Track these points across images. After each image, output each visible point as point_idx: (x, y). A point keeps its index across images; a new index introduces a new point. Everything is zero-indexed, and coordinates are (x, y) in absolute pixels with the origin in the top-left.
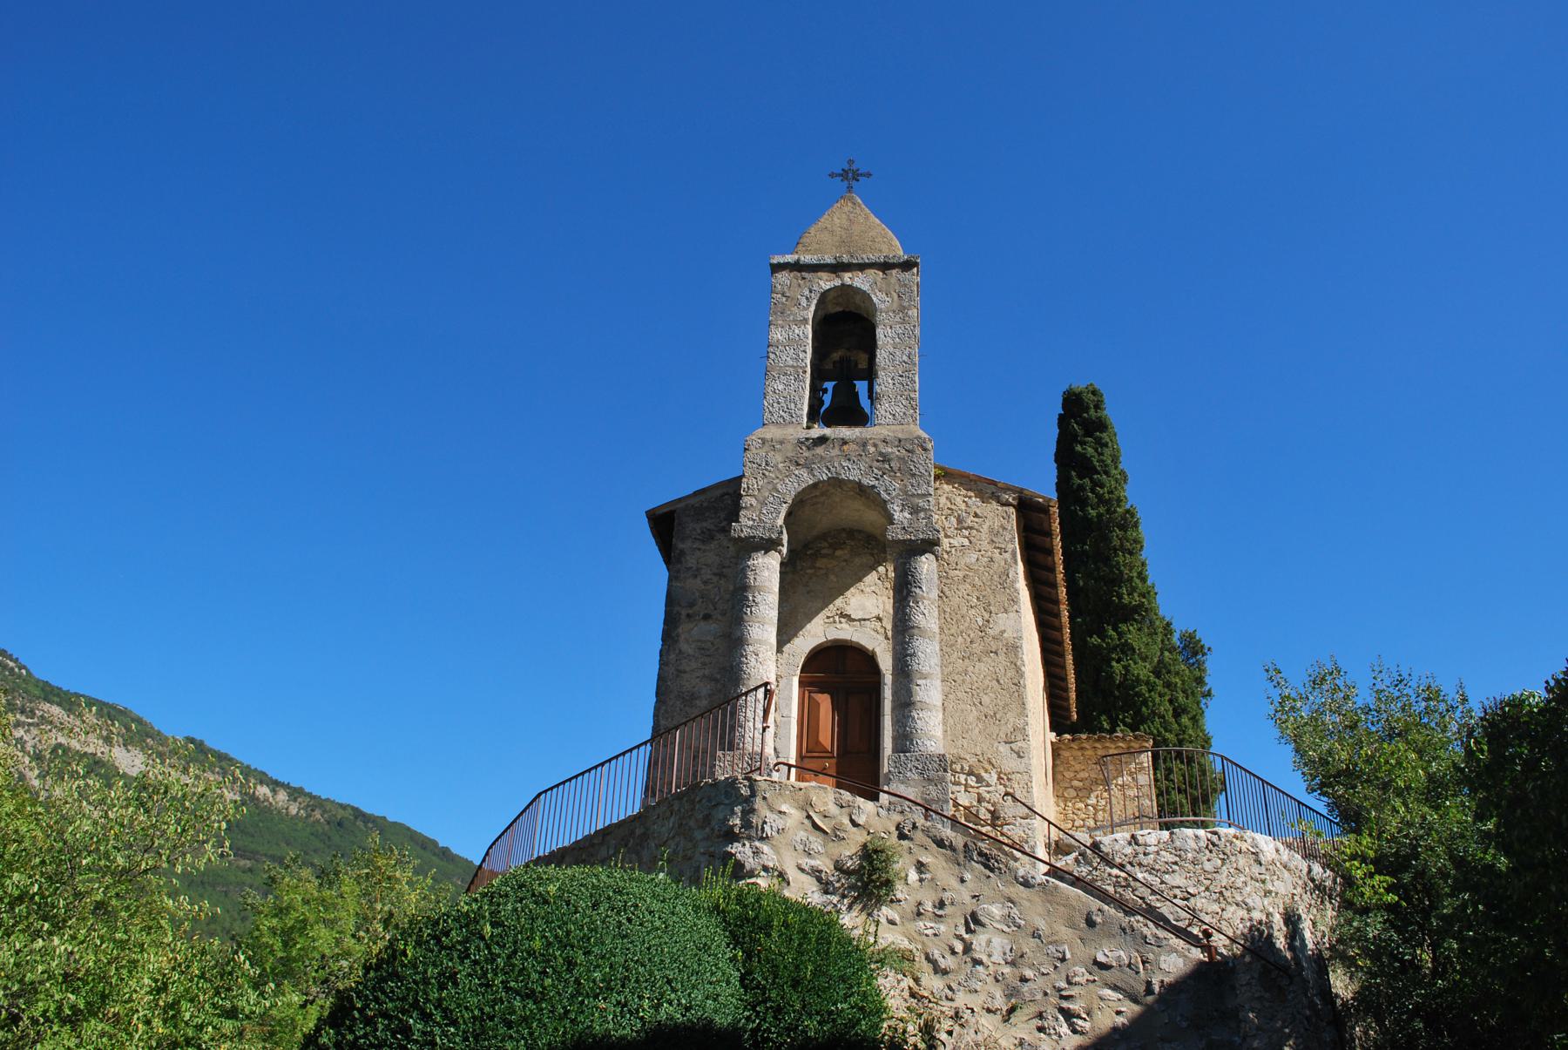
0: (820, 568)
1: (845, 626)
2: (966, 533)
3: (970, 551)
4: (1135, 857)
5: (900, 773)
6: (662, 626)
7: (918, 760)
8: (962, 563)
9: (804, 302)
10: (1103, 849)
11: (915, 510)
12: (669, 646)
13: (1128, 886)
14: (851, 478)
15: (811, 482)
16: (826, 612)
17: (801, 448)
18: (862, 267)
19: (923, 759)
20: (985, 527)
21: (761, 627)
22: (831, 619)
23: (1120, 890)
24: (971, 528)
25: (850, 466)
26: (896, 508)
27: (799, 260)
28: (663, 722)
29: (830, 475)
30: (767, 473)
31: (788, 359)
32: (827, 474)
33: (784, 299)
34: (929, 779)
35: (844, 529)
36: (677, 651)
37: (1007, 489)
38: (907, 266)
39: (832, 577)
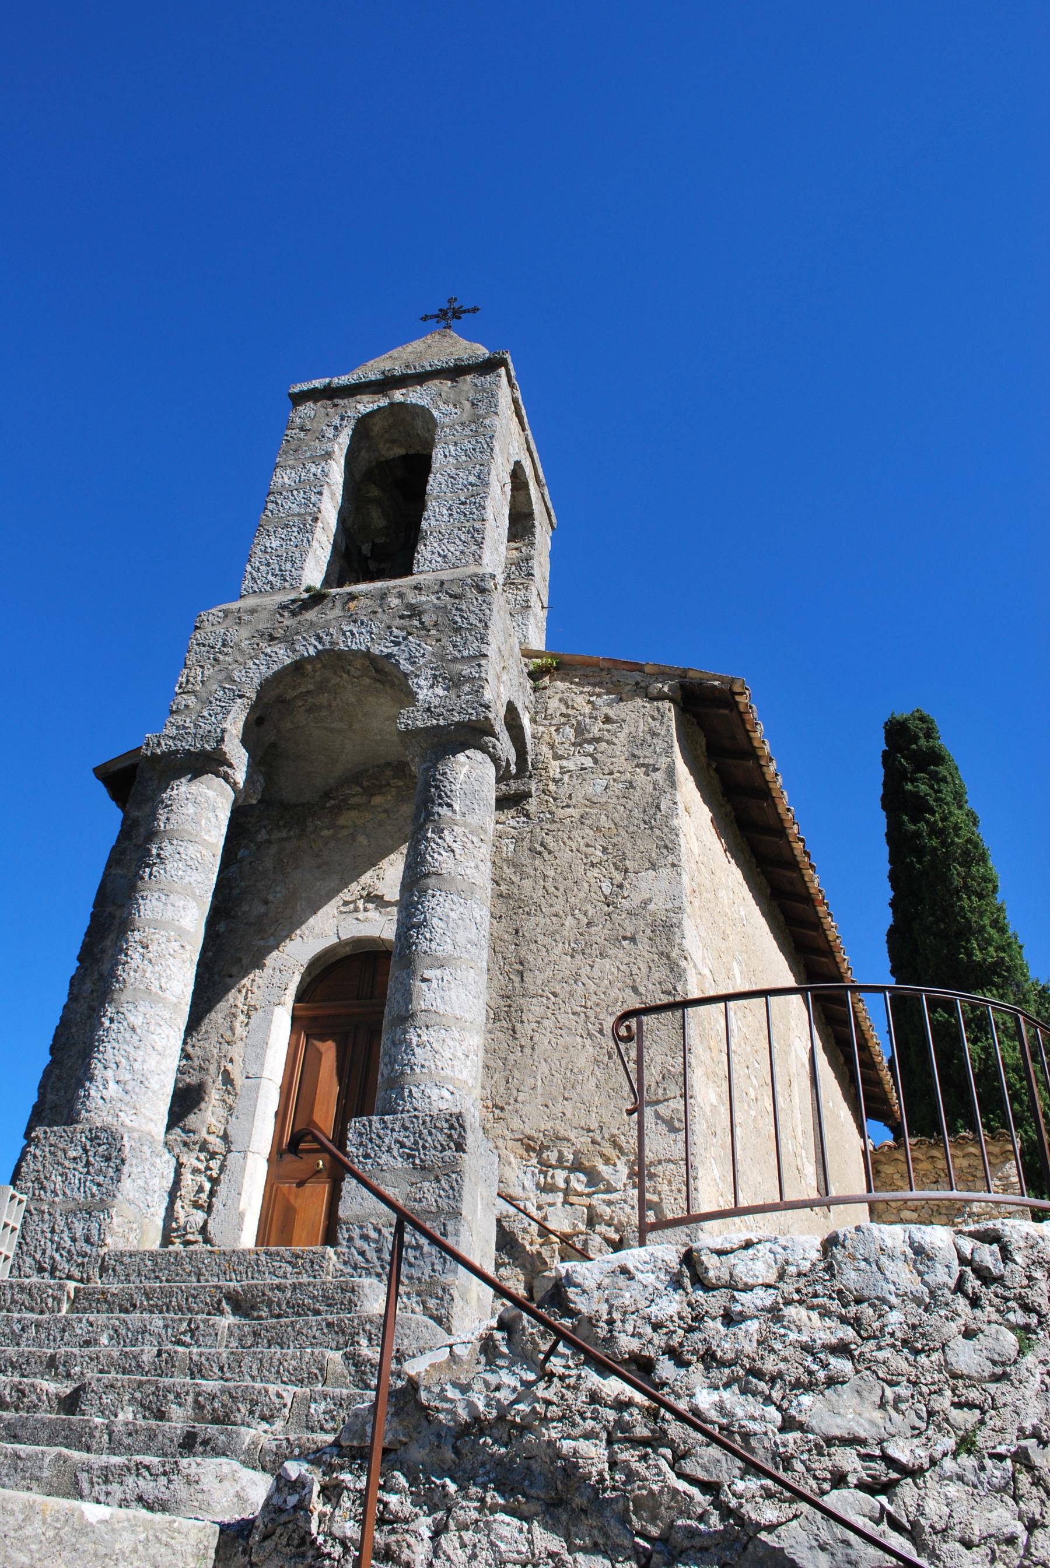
0: (344, 827)
1: (373, 914)
2: (590, 748)
3: (595, 776)
4: (690, 1330)
5: (367, 1156)
6: (82, 937)
7: (406, 1129)
8: (579, 797)
9: (330, 433)
10: (581, 1304)
11: (455, 683)
12: (86, 970)
13: (658, 1440)
14: (354, 647)
15: (288, 661)
16: (345, 895)
17: (282, 616)
18: (421, 378)
19: (418, 1125)
20: (622, 735)
21: (163, 898)
22: (352, 906)
23: (628, 1455)
24: (598, 740)
25: (355, 631)
26: (422, 683)
27: (329, 384)
28: (50, 1097)
29: (320, 647)
30: (221, 657)
31: (294, 506)
32: (315, 647)
33: (302, 434)
34: (423, 1168)
35: (389, 764)
36: (96, 977)
37: (662, 675)
38: (489, 366)
39: (362, 839)
